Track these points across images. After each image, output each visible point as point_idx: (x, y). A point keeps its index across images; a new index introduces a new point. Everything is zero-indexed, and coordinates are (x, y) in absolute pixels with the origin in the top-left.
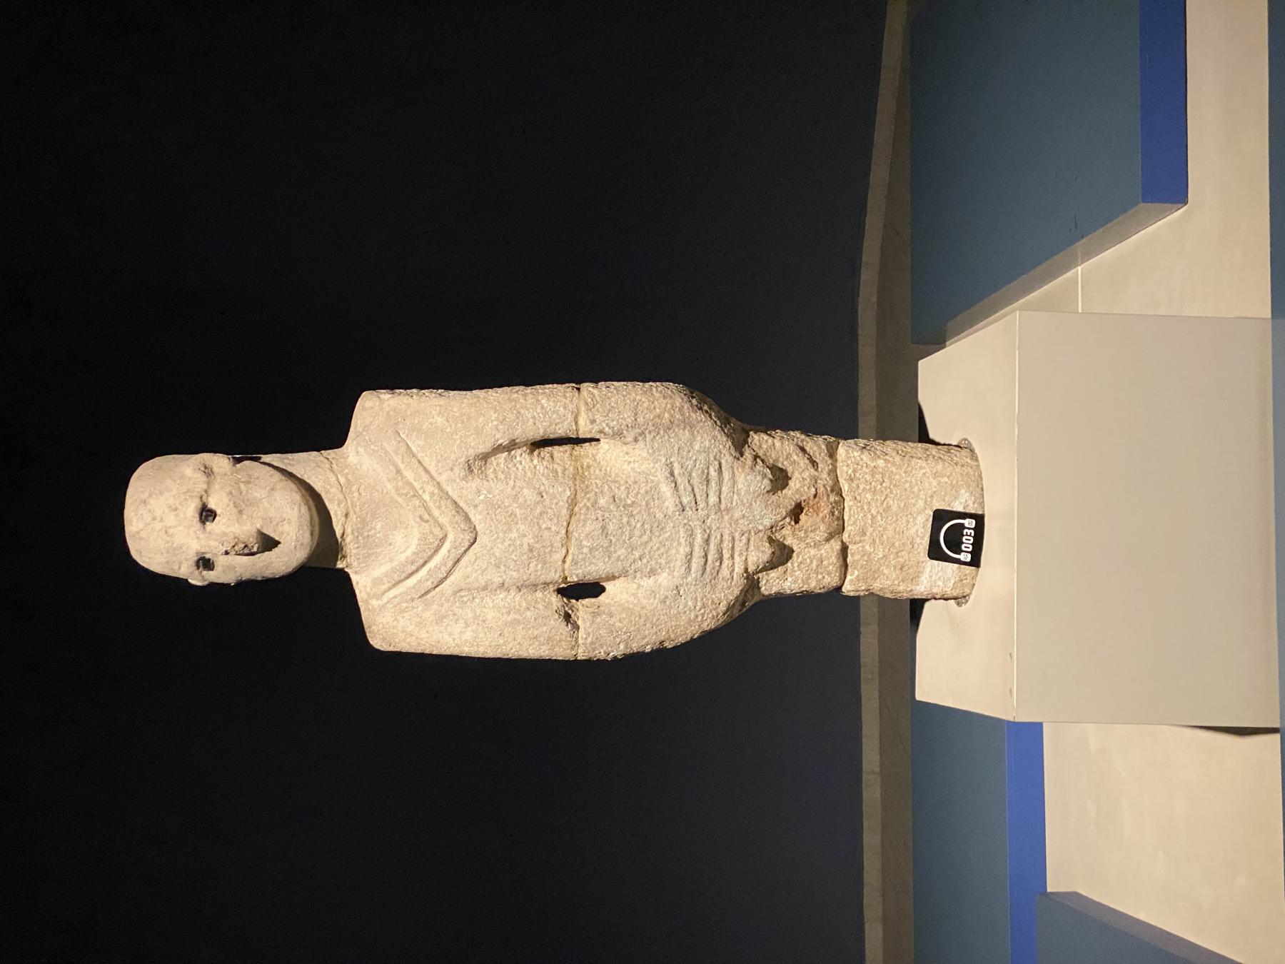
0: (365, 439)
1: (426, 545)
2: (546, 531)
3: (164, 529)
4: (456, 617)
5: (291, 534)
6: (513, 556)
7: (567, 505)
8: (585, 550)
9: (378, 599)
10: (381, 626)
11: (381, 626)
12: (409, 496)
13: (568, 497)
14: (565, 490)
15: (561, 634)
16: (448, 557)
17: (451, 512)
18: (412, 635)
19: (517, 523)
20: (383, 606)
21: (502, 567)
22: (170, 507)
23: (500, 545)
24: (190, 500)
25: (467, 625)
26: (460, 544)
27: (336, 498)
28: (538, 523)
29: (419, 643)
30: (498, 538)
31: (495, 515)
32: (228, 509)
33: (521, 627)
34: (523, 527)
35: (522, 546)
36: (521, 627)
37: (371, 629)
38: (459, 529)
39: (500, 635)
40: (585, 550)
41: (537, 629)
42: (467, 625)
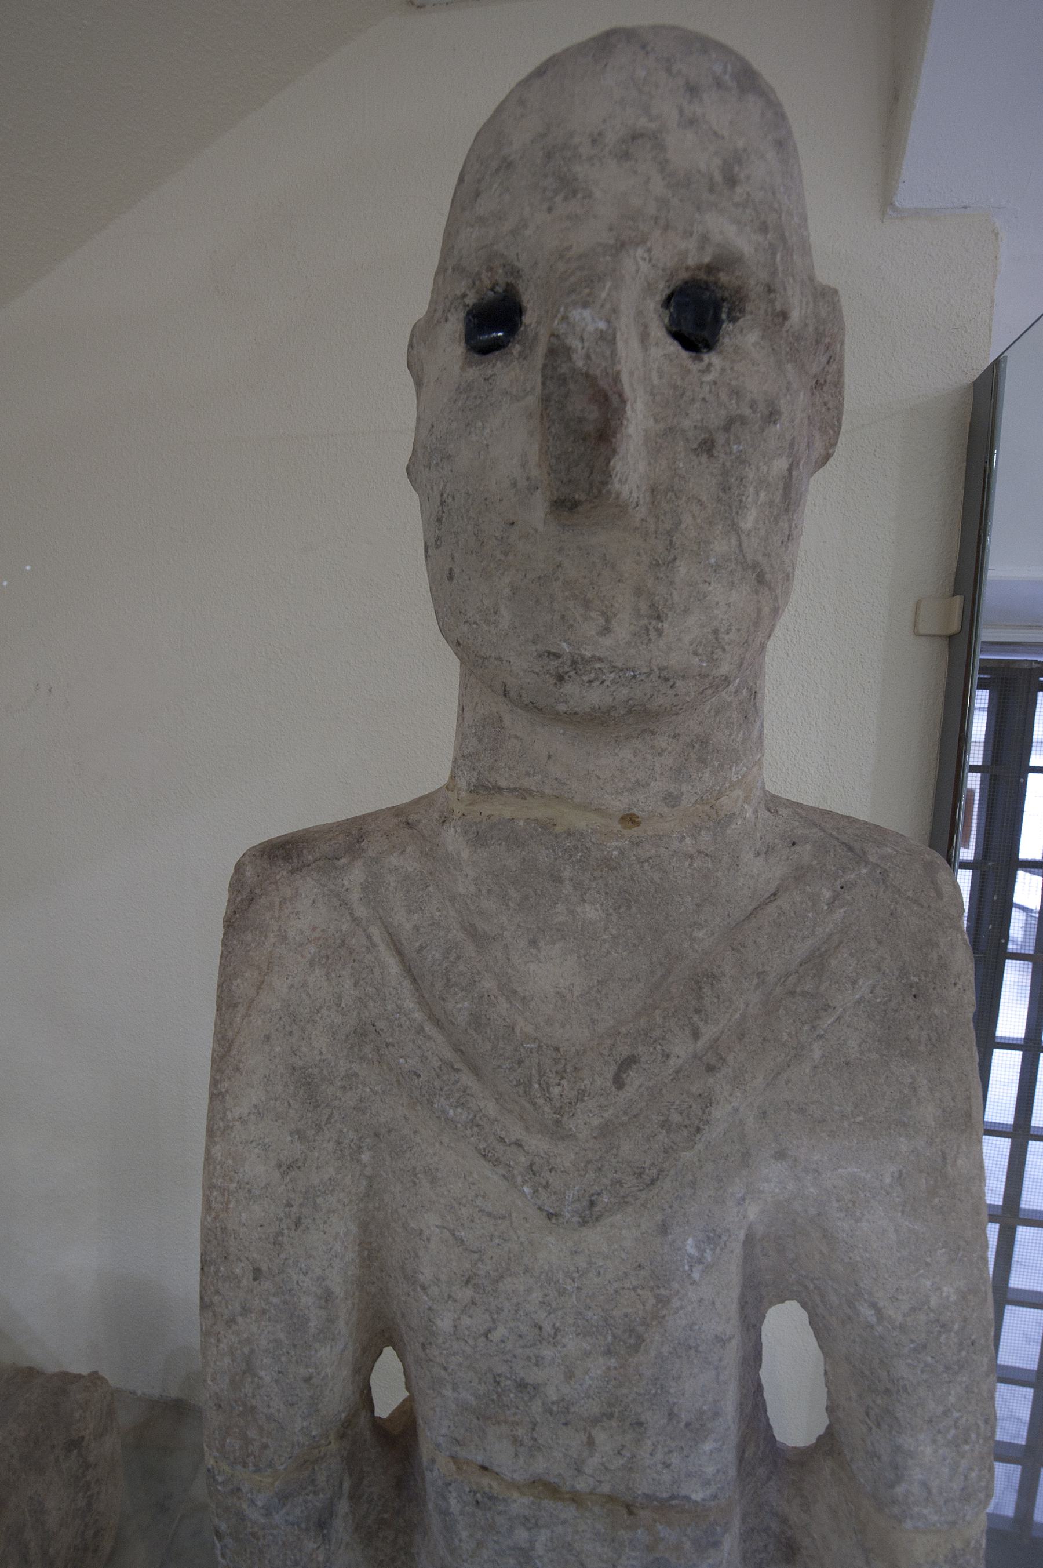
0: (844, 869)
1: (541, 1073)
2: (585, 1438)
3: (653, 126)
4: (311, 1133)
5: (607, 641)
6: (501, 1332)
7: (665, 1495)
8: (521, 1535)
9: (365, 888)
10: (288, 892)
11: (288, 892)
12: (696, 1018)
13: (687, 1498)
14: (707, 1483)
15: (265, 1447)
16: (502, 1140)
17: (653, 1164)
18: (259, 988)
19: (608, 1353)
20: (344, 903)
21: (468, 1293)
22: (739, 162)
23: (537, 1295)
24: (760, 238)
25: (287, 1167)
26: (546, 1186)
27: (684, 788)
28: (610, 1416)
29: (236, 1005)
30: (562, 1292)
31: (634, 1289)
32: (723, 395)
33: (282, 1336)
34: (597, 1367)
35: (537, 1365)
36: (282, 1336)
37: (280, 862)
38: (597, 1188)
39: (257, 1274)
40: (521, 1535)
41: (277, 1381)
42: (287, 1167)
